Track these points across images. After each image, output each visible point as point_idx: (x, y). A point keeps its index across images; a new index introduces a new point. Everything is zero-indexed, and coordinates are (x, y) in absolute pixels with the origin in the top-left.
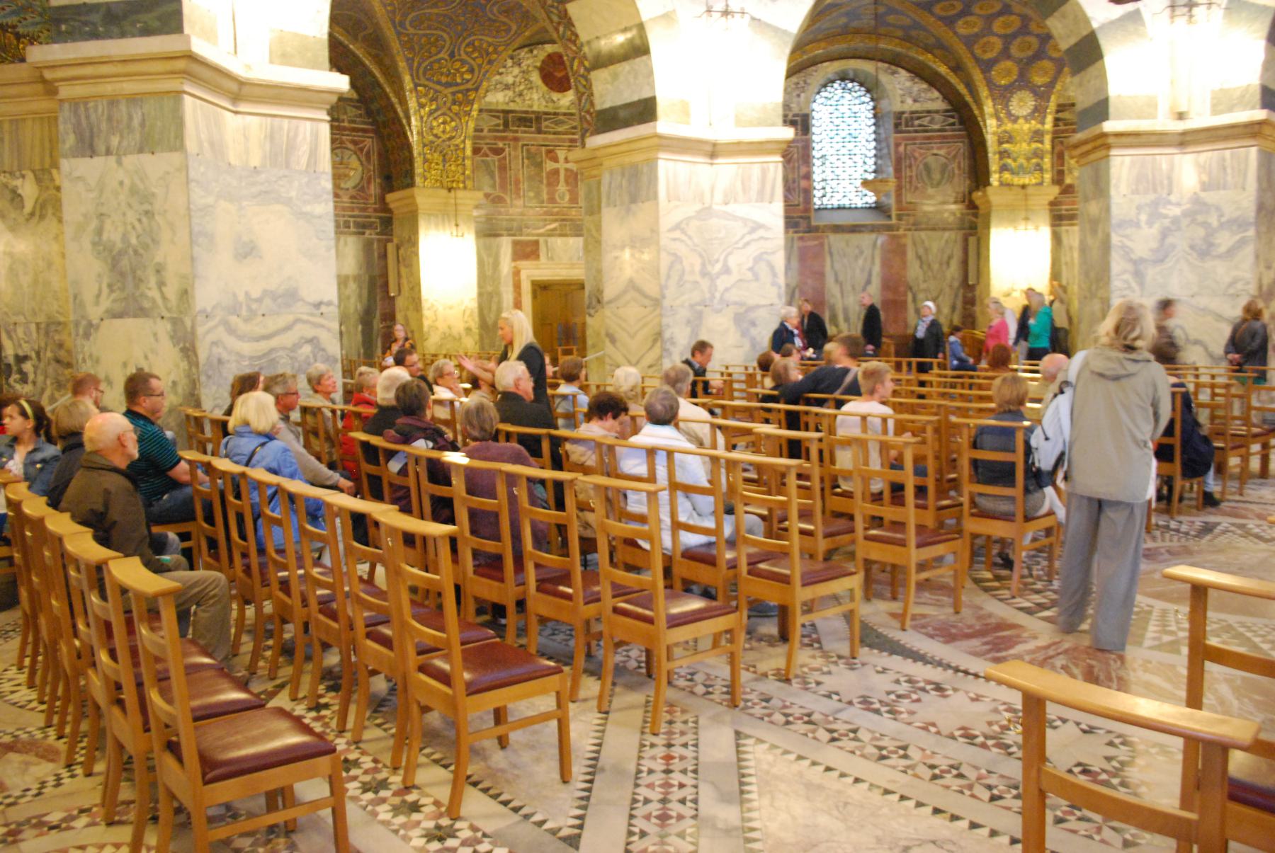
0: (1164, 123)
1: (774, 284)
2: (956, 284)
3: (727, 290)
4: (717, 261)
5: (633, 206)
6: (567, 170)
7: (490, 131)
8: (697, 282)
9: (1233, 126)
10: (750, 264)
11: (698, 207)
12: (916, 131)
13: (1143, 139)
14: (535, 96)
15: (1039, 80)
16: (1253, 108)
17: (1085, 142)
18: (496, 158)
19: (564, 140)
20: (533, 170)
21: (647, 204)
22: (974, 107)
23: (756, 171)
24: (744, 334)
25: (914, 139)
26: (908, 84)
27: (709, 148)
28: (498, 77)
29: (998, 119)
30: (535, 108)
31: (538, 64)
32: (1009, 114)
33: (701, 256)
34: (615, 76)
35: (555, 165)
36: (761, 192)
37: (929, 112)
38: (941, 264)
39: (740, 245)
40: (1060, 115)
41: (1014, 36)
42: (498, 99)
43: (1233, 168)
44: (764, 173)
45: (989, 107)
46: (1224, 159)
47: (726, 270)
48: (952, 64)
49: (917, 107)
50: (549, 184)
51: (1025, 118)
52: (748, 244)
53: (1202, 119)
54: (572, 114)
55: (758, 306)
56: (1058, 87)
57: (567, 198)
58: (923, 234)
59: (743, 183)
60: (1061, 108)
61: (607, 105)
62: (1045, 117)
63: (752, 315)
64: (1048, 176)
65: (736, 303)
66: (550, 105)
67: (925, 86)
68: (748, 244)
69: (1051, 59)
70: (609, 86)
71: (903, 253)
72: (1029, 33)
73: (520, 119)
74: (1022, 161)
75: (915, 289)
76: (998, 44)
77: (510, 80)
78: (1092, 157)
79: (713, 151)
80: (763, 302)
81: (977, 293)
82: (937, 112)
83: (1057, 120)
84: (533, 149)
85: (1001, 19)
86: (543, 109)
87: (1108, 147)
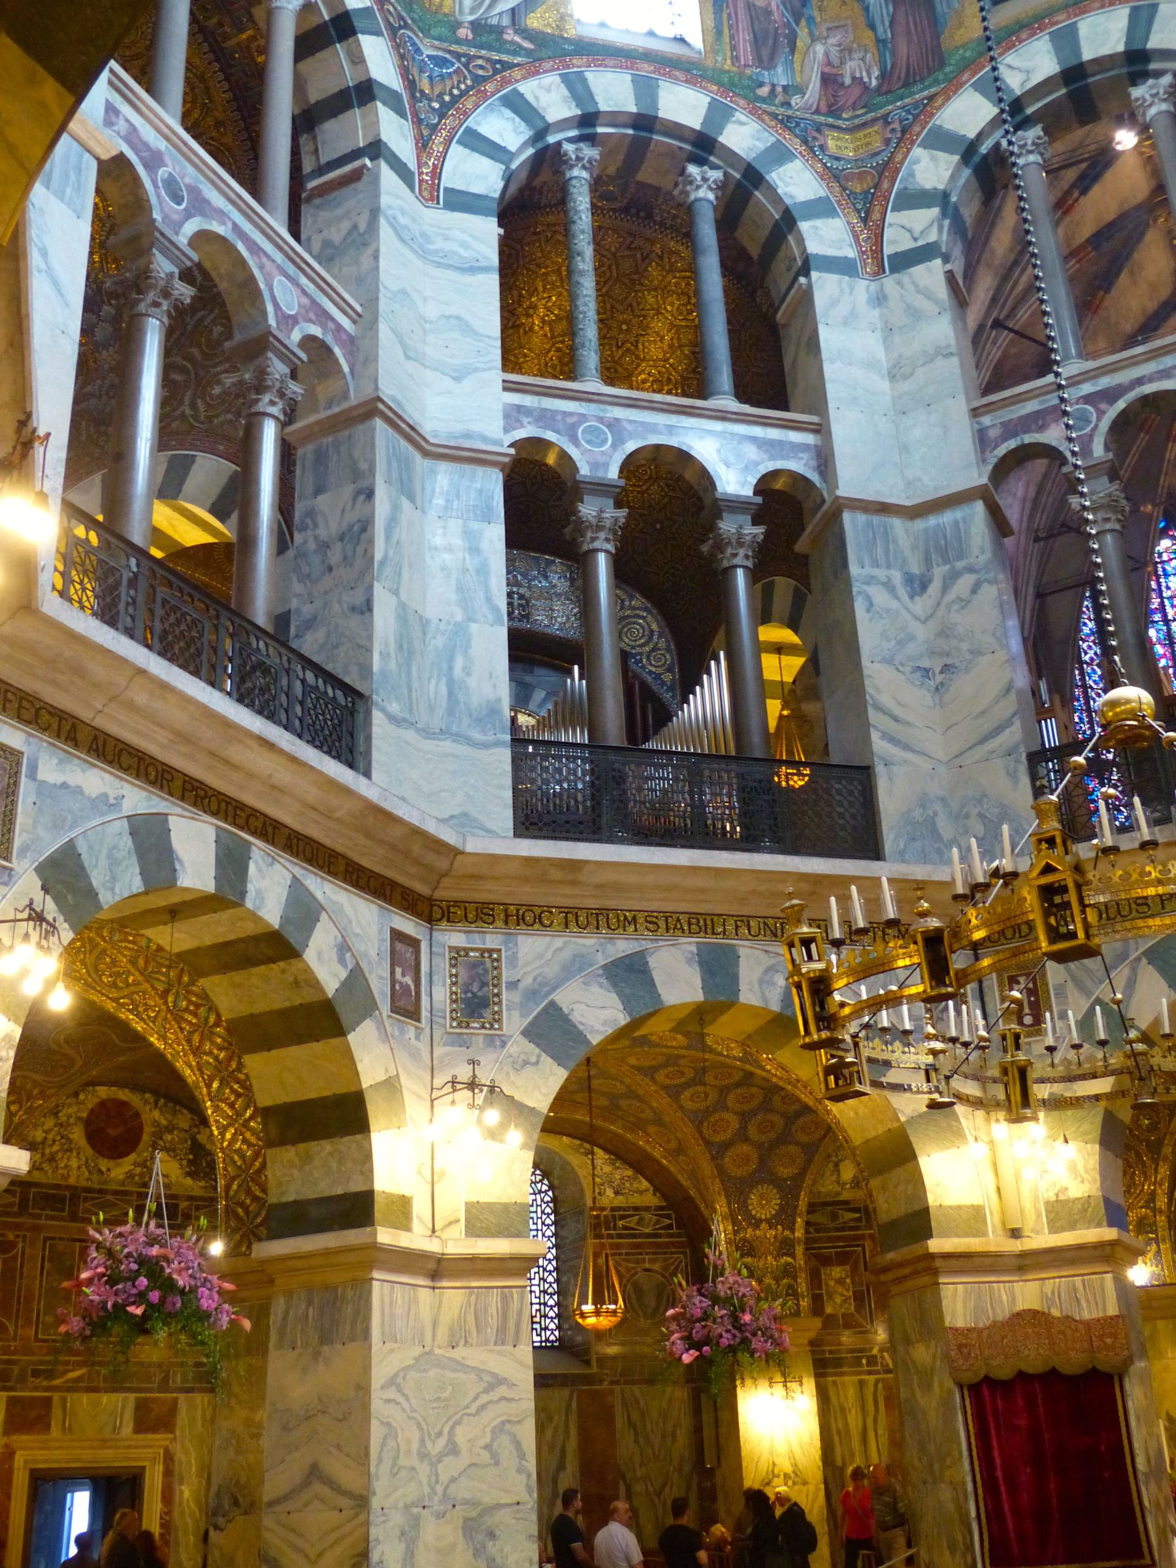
0: (994, 1241)
1: (519, 1471)
2: (687, 1468)
3: (453, 1480)
4: (440, 1434)
5: (326, 1349)
8: (413, 1469)
9: (1080, 1247)
10: (488, 1440)
11: (417, 1351)
12: (620, 1236)
13: (977, 1261)
14: (74, 1163)
15: (784, 1171)
16: (1099, 1225)
17: (901, 1265)
21: (350, 1346)
22: (702, 1207)
23: (494, 1299)
24: (477, 1553)
25: (618, 1246)
26: (607, 1169)
27: (431, 1265)
29: (735, 1223)
30: (72, 1181)
31: (84, 1115)
32: (749, 1217)
33: (419, 1425)
34: (307, 1159)
36: (502, 1331)
37: (636, 1209)
38: (664, 1436)
39: (473, 1409)
40: (812, 1218)
41: (754, 1113)
43: (1087, 1301)
44: (505, 1301)
45: (721, 1206)
46: (1075, 1290)
47: (453, 1450)
48: (673, 1145)
49: (620, 1201)
51: (768, 1221)
52: (483, 1407)
53: (1042, 1239)
54: (125, 1193)
55: (499, 1506)
56: (808, 1180)
58: (636, 1389)
59: (476, 1319)
60: (812, 1208)
61: (291, 1197)
62: (794, 1223)
63: (489, 1521)
64: (804, 1303)
65: (466, 1502)
66: (95, 1177)
67: (630, 1172)
68: (483, 1407)
69: (798, 1143)
70: (296, 1172)
71: (610, 1420)
72: (771, 1110)
73: (47, 1197)
74: (768, 1280)
75: (628, 1476)
76: (734, 1122)
78: (910, 1284)
79: (437, 1268)
80: (506, 1499)
81: (719, 1481)
82: (647, 1209)
83: (808, 1223)
85: (739, 1091)
86: (83, 1183)
87: (936, 1273)
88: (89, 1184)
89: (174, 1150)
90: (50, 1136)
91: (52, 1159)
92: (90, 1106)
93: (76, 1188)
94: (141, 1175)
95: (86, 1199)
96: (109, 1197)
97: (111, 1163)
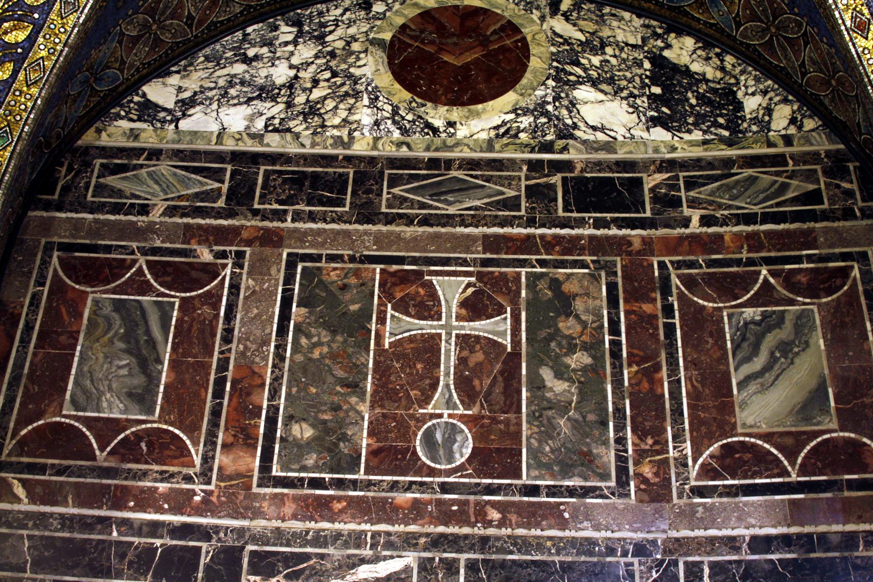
6: (464, 341)
7: (171, 211)
14: (365, 116)
18: (176, 298)
19: (467, 243)
20: (322, 344)
28: (239, 68)
30: (361, 147)
31: (387, 36)
35: (427, 327)
42: (231, 122)
50: (385, 394)
54: (497, 164)
57: (464, 449)
66: (417, 139)
73: (298, 180)
77: (281, 74)
84: (333, 273)
86: (387, 150)
88: (404, 151)
89: (611, 81)
90: (306, 75)
91: (312, 110)
92: (400, 21)
93: (372, 160)
94: (534, 130)
95: (394, 181)
96: (454, 173)
97: (456, 114)
